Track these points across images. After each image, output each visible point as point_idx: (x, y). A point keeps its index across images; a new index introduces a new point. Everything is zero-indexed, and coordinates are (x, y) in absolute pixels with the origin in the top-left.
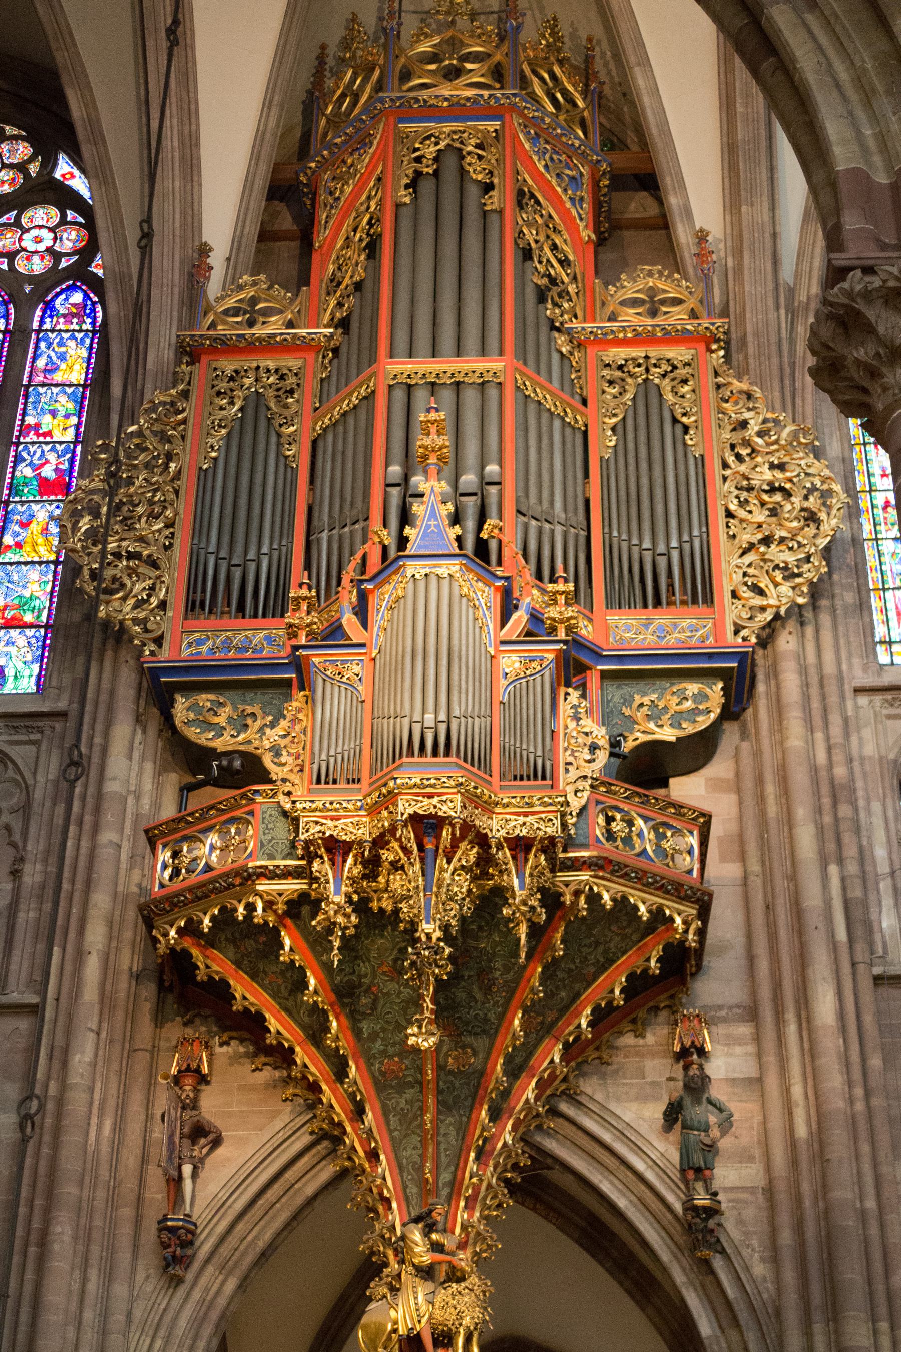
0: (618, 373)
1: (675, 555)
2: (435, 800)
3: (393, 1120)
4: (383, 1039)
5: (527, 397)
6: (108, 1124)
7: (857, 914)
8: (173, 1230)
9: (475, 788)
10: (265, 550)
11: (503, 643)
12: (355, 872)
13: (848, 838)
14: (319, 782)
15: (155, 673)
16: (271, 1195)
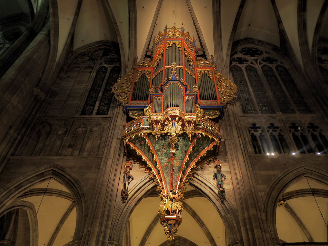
0: (200, 72)
1: (210, 94)
2: (175, 113)
3: (165, 174)
4: (163, 160)
5: (187, 72)
6: (113, 174)
7: (245, 146)
8: (124, 192)
9: (182, 112)
10: (145, 92)
11: (185, 94)
12: (160, 126)
13: (242, 135)
14: (154, 112)
15: (126, 107)
16: (142, 189)
